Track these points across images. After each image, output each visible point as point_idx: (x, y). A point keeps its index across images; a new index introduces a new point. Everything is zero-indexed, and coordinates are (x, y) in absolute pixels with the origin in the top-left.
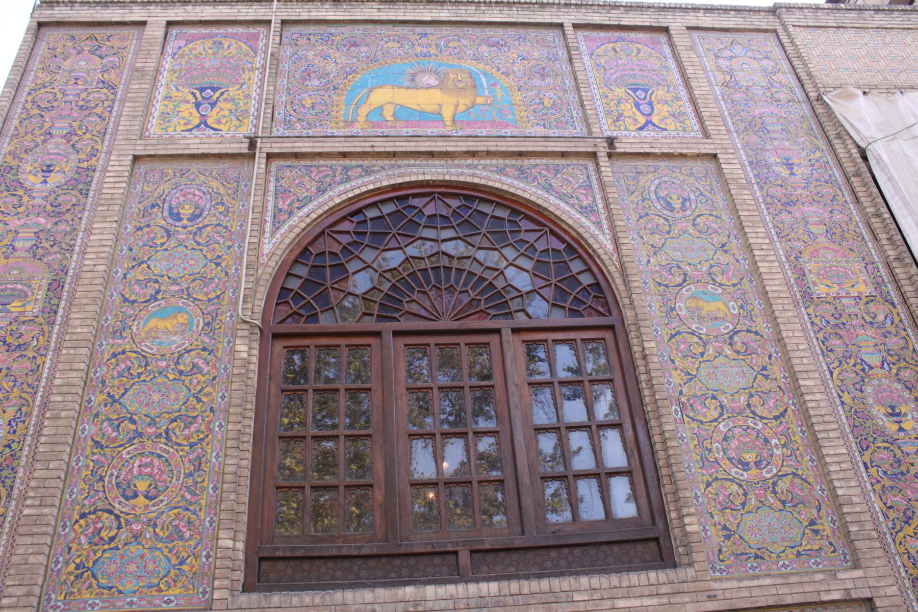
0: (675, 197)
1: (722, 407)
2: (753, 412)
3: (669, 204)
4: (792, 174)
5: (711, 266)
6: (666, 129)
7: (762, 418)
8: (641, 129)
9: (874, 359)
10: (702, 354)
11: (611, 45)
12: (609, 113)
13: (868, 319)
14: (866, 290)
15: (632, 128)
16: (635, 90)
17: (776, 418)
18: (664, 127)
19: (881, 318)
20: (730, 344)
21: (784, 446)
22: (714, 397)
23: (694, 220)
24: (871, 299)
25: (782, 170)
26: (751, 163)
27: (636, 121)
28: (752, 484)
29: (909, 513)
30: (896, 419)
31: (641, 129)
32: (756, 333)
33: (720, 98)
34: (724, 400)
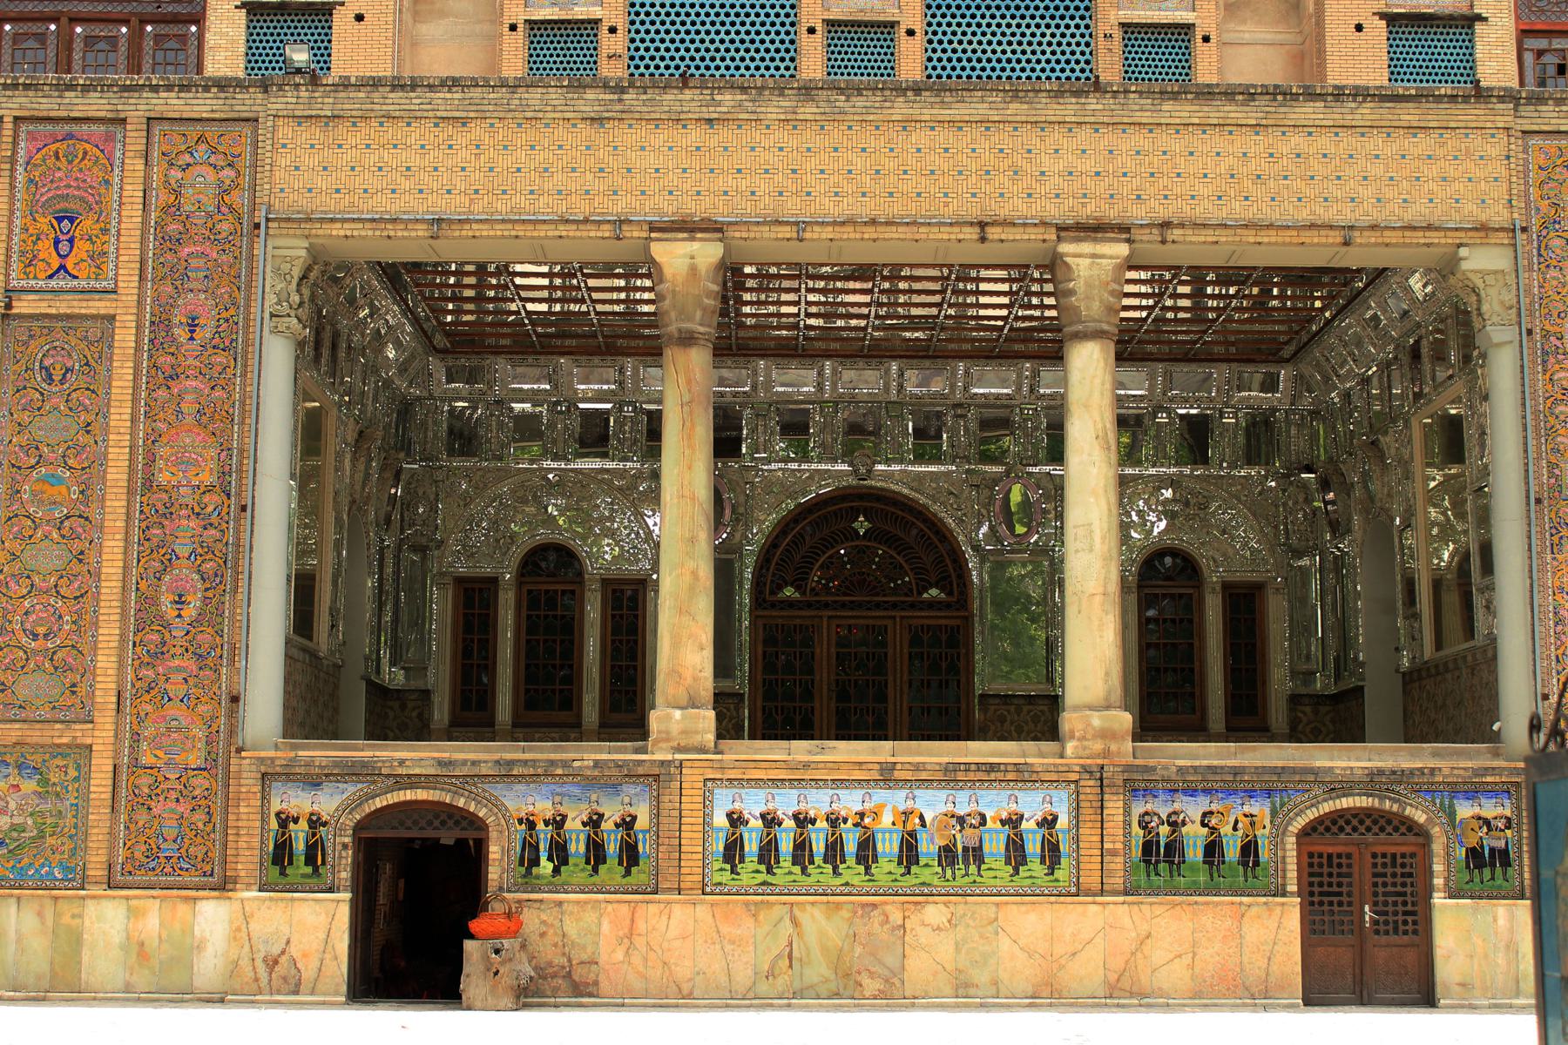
0: (58, 367)
1: (32, 585)
2: (58, 592)
3: (50, 376)
4: (192, 339)
5: (69, 448)
6: (76, 277)
7: (63, 597)
8: (51, 277)
9: (183, 551)
10: (31, 537)
11: (54, 147)
12: (23, 253)
13: (197, 510)
14: (208, 478)
15: (43, 275)
16: (60, 220)
17: (76, 598)
18: (76, 274)
19: (210, 509)
20: (59, 529)
21: (74, 622)
22: (28, 577)
23: (69, 395)
24: (209, 489)
25: (182, 333)
26: (153, 323)
27: (49, 264)
28: (36, 652)
29: (153, 685)
30: (179, 606)
31: (51, 277)
32: (87, 519)
33: (152, 230)
34: (36, 579)
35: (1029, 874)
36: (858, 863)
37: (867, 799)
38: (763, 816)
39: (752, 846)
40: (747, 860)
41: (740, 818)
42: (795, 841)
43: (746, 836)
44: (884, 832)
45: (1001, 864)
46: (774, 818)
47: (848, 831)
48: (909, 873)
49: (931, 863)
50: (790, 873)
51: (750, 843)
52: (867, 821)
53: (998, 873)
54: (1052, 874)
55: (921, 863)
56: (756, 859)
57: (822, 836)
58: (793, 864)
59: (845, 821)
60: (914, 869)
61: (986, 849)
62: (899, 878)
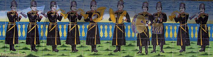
35: (190, 51)
36: (88, 43)
37: (94, 4)
38: (29, 15)
39: (22, 33)
40: (20, 41)
41: (15, 16)
42: (49, 30)
43: (19, 27)
44: (104, 24)
45: (174, 45)
46: (36, 16)
47: (81, 24)
48: (119, 50)
49: (133, 44)
50: (46, 50)
51: (22, 32)
52: (93, 18)
53: (173, 50)
54: (204, 50)
55: (127, 44)
56: (25, 41)
57: (65, 27)
58: (48, 44)
59: (80, 18)
60: (123, 48)
61: (166, 35)
62: (113, 53)
